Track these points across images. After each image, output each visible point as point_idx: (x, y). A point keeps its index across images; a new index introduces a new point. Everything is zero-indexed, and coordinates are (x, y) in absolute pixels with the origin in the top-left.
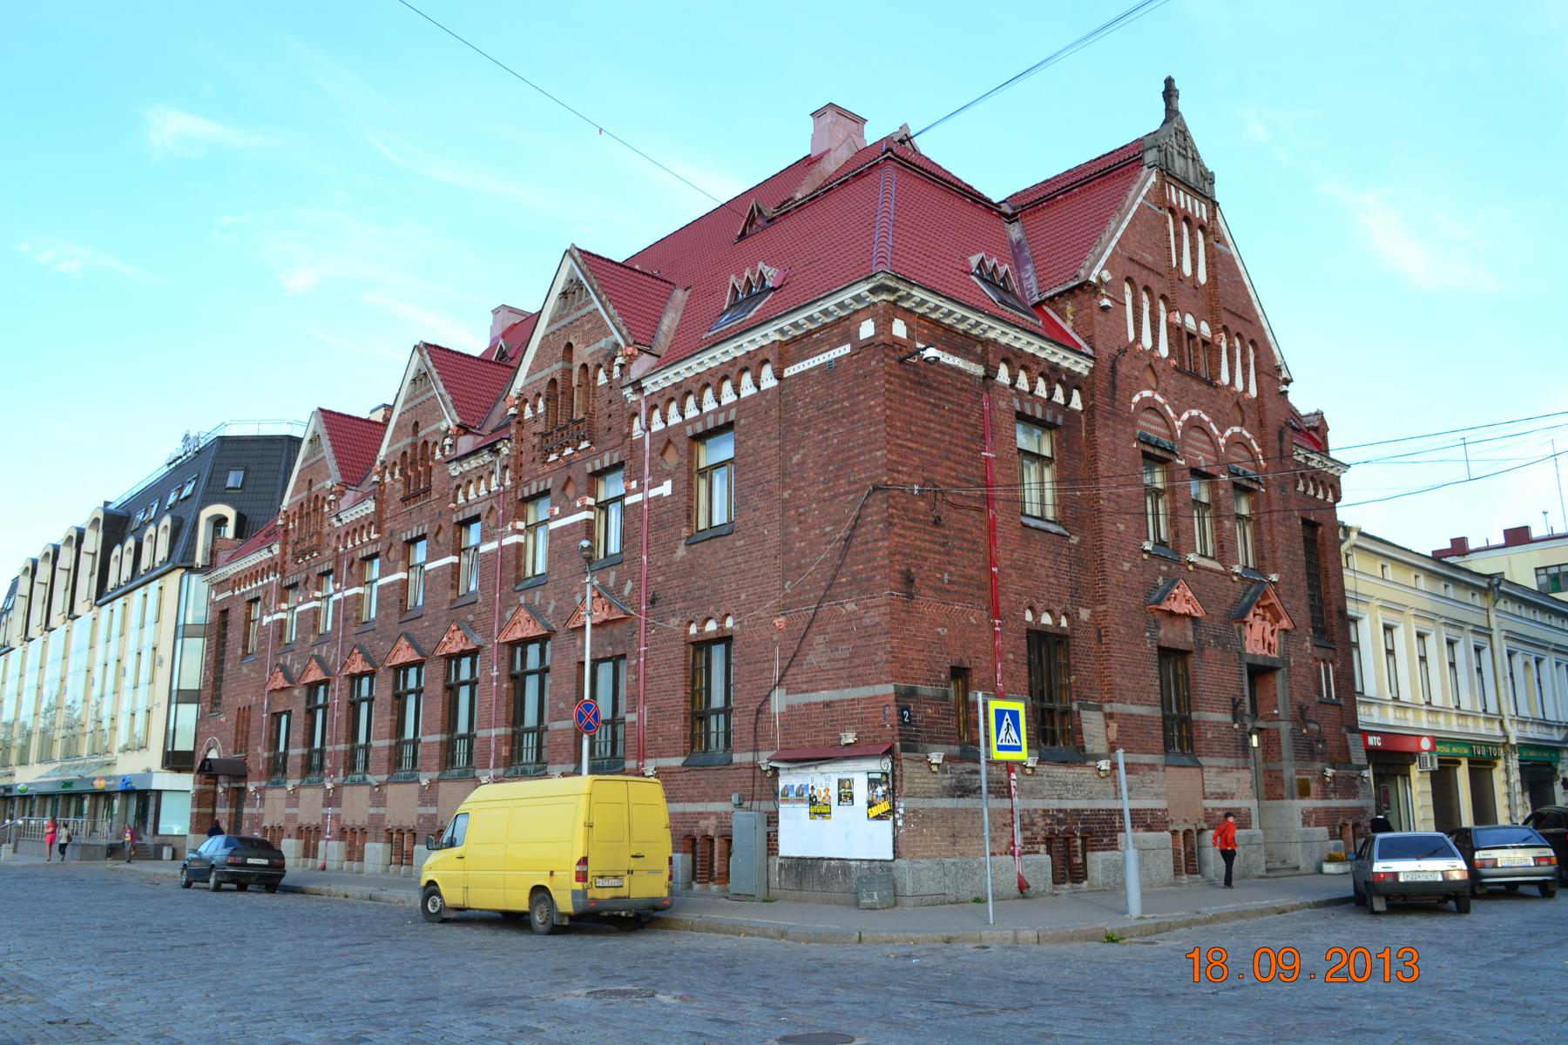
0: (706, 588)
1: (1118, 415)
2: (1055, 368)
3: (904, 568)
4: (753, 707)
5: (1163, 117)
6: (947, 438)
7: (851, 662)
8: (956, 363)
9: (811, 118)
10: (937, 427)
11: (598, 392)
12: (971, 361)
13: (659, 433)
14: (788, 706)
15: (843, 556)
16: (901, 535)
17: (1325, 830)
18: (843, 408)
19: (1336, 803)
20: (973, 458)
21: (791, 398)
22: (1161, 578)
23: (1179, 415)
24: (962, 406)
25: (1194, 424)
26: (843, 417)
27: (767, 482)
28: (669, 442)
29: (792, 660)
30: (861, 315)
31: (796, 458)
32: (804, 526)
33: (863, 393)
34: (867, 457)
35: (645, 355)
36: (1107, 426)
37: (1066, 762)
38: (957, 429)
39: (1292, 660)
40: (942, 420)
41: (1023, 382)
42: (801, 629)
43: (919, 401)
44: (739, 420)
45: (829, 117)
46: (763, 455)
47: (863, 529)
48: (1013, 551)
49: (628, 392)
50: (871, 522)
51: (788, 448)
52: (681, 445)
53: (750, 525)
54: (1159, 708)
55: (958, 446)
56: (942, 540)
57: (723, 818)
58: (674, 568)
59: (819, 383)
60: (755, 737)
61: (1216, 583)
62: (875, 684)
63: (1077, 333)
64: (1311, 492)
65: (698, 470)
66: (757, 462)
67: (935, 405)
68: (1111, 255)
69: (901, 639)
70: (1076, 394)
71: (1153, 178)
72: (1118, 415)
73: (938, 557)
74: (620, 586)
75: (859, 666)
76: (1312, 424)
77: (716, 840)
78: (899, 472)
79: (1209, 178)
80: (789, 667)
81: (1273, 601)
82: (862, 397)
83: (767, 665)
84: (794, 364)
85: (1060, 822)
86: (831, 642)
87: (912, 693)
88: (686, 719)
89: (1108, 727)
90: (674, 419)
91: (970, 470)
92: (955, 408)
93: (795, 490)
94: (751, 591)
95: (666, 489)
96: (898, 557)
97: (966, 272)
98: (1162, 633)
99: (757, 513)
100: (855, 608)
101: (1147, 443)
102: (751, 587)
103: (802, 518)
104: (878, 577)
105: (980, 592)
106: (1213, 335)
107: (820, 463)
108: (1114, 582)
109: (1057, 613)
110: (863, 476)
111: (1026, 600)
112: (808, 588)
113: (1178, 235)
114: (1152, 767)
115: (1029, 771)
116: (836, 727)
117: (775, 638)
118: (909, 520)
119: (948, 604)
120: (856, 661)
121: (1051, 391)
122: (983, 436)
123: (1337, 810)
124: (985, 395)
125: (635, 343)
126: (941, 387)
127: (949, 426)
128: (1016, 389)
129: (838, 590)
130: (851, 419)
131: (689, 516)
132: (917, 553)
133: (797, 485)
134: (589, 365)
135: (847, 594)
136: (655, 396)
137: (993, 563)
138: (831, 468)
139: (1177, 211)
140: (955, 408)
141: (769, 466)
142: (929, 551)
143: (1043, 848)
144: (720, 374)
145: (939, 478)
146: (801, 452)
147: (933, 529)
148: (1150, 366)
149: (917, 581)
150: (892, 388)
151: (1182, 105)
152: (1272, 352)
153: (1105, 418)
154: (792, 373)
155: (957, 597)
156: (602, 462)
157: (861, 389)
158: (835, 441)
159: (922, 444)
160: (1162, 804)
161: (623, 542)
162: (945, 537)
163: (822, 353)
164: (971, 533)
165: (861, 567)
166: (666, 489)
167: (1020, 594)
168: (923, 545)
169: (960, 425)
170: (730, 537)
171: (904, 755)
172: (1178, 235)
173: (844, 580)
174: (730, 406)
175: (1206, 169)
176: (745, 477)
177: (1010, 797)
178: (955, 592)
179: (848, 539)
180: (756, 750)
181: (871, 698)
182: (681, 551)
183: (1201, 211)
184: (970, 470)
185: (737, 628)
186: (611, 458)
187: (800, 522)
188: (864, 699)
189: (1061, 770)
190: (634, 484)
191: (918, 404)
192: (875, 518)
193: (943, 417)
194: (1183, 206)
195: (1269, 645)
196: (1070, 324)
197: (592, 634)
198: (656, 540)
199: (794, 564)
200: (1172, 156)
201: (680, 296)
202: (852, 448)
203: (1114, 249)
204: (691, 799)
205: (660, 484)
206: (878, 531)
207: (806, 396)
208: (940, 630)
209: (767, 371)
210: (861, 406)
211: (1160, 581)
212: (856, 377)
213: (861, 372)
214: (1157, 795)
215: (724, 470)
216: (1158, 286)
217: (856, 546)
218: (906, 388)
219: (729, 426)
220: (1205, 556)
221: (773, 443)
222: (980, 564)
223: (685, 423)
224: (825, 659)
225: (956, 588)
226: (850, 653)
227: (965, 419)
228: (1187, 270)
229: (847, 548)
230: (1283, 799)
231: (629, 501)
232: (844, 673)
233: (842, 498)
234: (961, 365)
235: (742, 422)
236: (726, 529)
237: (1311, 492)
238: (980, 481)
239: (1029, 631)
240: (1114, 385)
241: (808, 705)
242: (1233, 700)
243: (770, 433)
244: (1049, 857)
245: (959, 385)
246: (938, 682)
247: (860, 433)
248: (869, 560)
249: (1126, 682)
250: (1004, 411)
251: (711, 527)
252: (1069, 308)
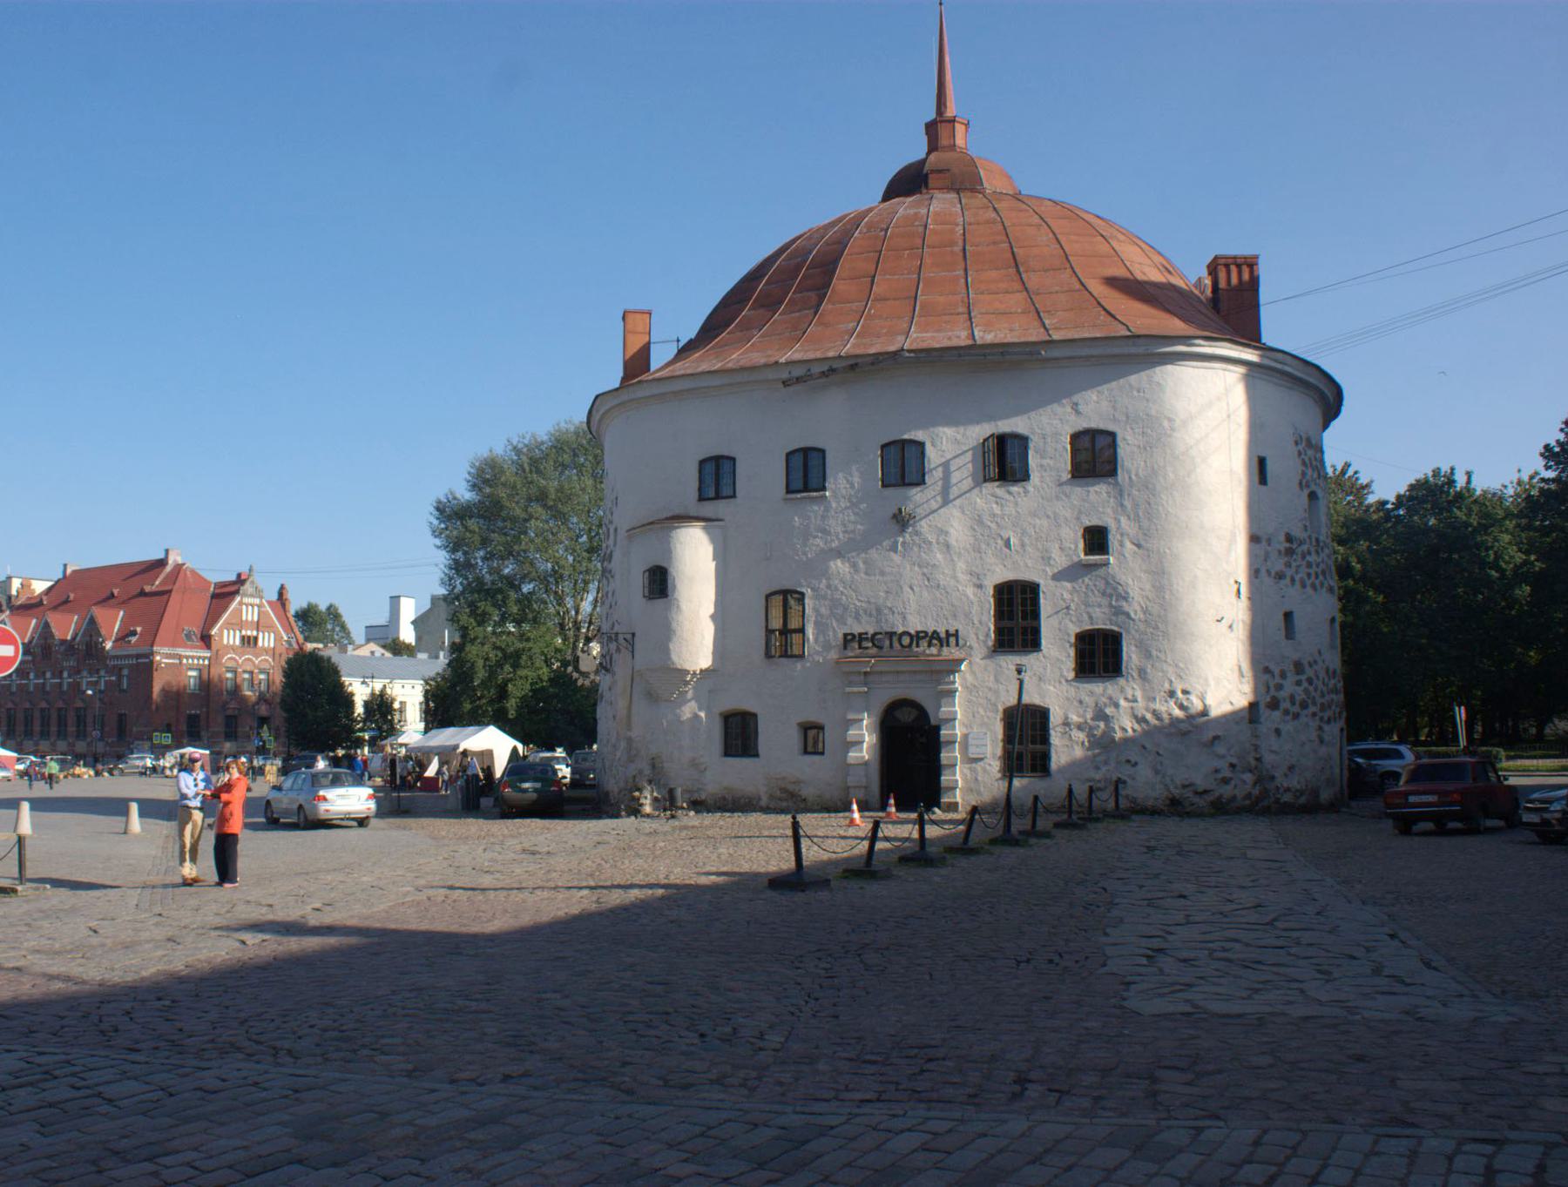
25: (246, 659)
95: (114, 678)
166: (114, 678)
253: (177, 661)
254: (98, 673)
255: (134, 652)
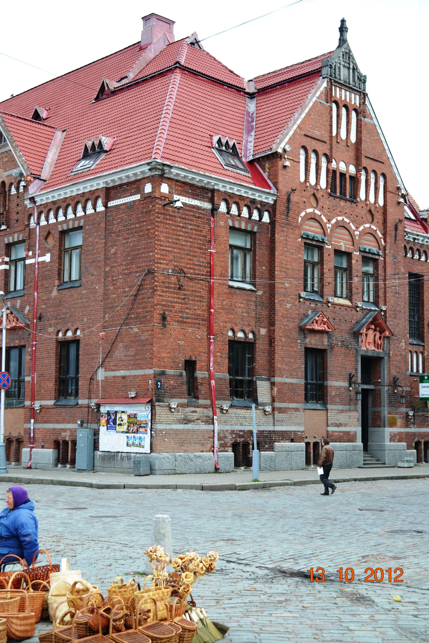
0: (67, 313)
1: (291, 225)
2: (253, 201)
3: (161, 312)
4: (89, 376)
5: (337, 44)
6: (189, 244)
7: (135, 357)
8: (196, 204)
9: (142, 21)
10: (184, 238)
11: (11, 198)
12: (205, 201)
13: (44, 226)
14: (105, 377)
15: (133, 304)
16: (160, 296)
17: (405, 444)
18: (136, 228)
19: (413, 430)
20: (203, 253)
21: (112, 218)
22: (310, 311)
23: (329, 221)
24: (199, 226)
26: (136, 232)
27: (98, 261)
28: (49, 233)
29: (108, 355)
30: (146, 180)
31: (113, 251)
32: (115, 286)
33: (145, 221)
34: (146, 255)
35: (37, 181)
36: (283, 231)
37: (246, 407)
38: (195, 239)
39: (391, 353)
40: (186, 235)
41: (234, 210)
42: (112, 339)
43: (174, 225)
44: (85, 226)
45: (153, 21)
46: (97, 247)
47: (143, 292)
48: (224, 300)
49: (27, 202)
50: (146, 288)
51: (109, 245)
52: (55, 235)
53: (89, 283)
54: (304, 380)
55: (195, 247)
56: (183, 297)
57: (73, 432)
58: (51, 302)
59: (125, 212)
60: (89, 392)
61: (345, 312)
62: (145, 369)
63: (270, 180)
64: (416, 257)
65: (65, 249)
66: (93, 250)
67: (183, 227)
68: (293, 135)
69: (159, 347)
70: (266, 214)
71: (325, 85)
72: (291, 225)
73: (180, 305)
74: (22, 308)
75: (138, 359)
76: (423, 217)
77: (70, 443)
78: (161, 263)
79: (362, 80)
80: (106, 357)
81: (380, 321)
82: (145, 224)
83: (95, 356)
84: (113, 200)
85: (240, 436)
86: (126, 346)
87: (163, 373)
88: (56, 381)
89: (272, 389)
90: (52, 220)
91: (201, 260)
92: (194, 227)
93: (112, 267)
94: (89, 317)
96: (158, 307)
97: (209, 147)
98: (307, 340)
99: (93, 277)
100: (137, 330)
101: (307, 238)
102: (89, 315)
103: (115, 282)
104: (149, 316)
105: (203, 322)
106: (357, 172)
107: (124, 255)
108: (280, 314)
109: (247, 331)
110: (144, 264)
111: (229, 325)
112: (116, 318)
113: (339, 116)
114: (297, 410)
115: (225, 412)
116: (127, 388)
117: (100, 342)
118: (165, 288)
119: (185, 329)
120: (137, 357)
121: (251, 214)
122: (210, 241)
123: (414, 434)
124: (212, 219)
125: (31, 174)
126: (187, 217)
127: (190, 238)
128: (231, 215)
129: (130, 321)
130: (139, 234)
131: (59, 274)
132: (169, 304)
133: (113, 265)
134: (6, 182)
135: (134, 324)
136: (42, 206)
137: (210, 307)
138: (129, 258)
139: (339, 102)
140: (194, 227)
141: (99, 253)
142: (176, 302)
143: (230, 449)
144: (76, 200)
145: (183, 265)
146: (115, 247)
147: (178, 291)
148: (314, 195)
149: (168, 318)
150: (159, 220)
151: (349, 36)
152: (396, 179)
153: (282, 227)
154: (112, 205)
155: (190, 325)
156: (13, 239)
157: (145, 219)
158: (131, 244)
159: (175, 248)
160: (302, 429)
161: (24, 285)
162: (185, 295)
163: (126, 197)
164: (200, 292)
165: (141, 310)
166: (47, 258)
167: (226, 322)
168: (172, 300)
169: (196, 237)
170: (79, 288)
171: (157, 404)
172: (339, 116)
173: (133, 316)
174: (81, 217)
175: (361, 75)
176: (88, 257)
177: (213, 424)
178: (189, 323)
179: (136, 296)
180: (90, 398)
181: (143, 375)
182: (55, 293)
183: (355, 100)
184: (201, 260)
185: (82, 336)
186: (18, 237)
187: (113, 285)
188: (140, 376)
189: (243, 411)
190: (30, 253)
191: (173, 227)
192: (148, 286)
193: (187, 233)
194: (343, 98)
195: (378, 344)
196: (267, 174)
197: (6, 335)
198: (42, 285)
199: (110, 305)
200: (339, 68)
201: (59, 136)
202: (139, 250)
203: (296, 131)
204: (58, 422)
205: (44, 255)
206: (149, 293)
207: (118, 219)
208: (180, 342)
209: (100, 202)
210: (144, 228)
211: (310, 312)
212: (142, 213)
213: (144, 210)
214: (298, 424)
215: (78, 251)
216: (322, 148)
217: (139, 300)
218: (167, 219)
219: (80, 228)
220: (341, 297)
221: (102, 241)
222: (204, 308)
223: (58, 223)
224: (123, 355)
225: (190, 321)
226: (135, 353)
227: (199, 233)
228: (343, 135)
229: (135, 300)
230: (380, 427)
231: (28, 262)
232: (132, 362)
233: (133, 274)
234: (199, 204)
235: (87, 227)
236: (77, 284)
237: (416, 257)
238: (206, 265)
239: (230, 341)
240: (288, 208)
241: (114, 377)
242: (350, 375)
243: (100, 235)
244: (233, 453)
245: (197, 215)
246: (177, 368)
247: (143, 242)
248: (144, 308)
249: (284, 366)
250: (222, 227)
251: (71, 281)
252: (267, 165)
253: (208, 206)
254: (8, 254)
255: (100, 184)
